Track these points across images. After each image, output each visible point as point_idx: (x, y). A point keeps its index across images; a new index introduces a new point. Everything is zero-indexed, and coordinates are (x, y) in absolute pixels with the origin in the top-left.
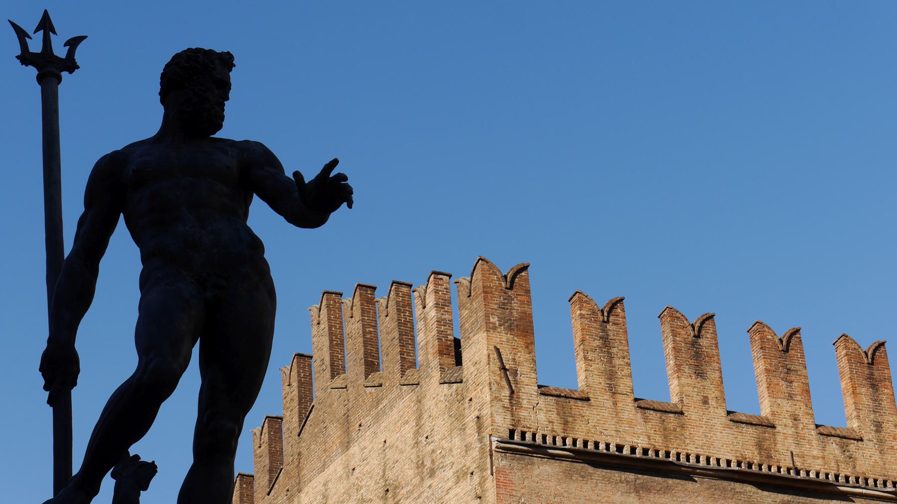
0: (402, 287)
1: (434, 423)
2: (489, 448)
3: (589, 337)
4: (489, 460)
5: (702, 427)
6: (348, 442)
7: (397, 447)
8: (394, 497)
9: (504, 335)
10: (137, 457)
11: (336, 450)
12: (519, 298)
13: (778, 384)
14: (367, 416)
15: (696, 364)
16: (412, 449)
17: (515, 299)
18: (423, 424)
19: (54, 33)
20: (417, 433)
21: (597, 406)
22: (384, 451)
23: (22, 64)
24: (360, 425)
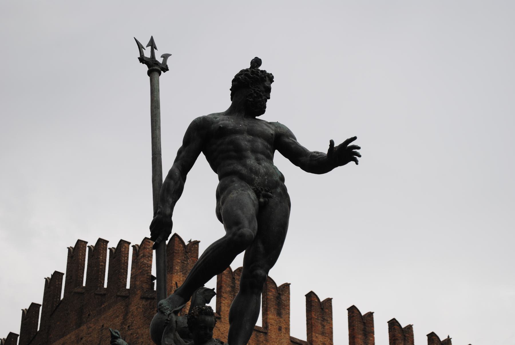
0: (126, 243)
1: (134, 319)
3: (225, 286)
5: (276, 343)
9: (182, 277)
12: (192, 259)
13: (317, 326)
15: (278, 309)
17: (190, 259)
19: (156, 49)
20: (123, 323)
21: (225, 323)
22: (102, 330)
23: (140, 63)
24: (89, 315)
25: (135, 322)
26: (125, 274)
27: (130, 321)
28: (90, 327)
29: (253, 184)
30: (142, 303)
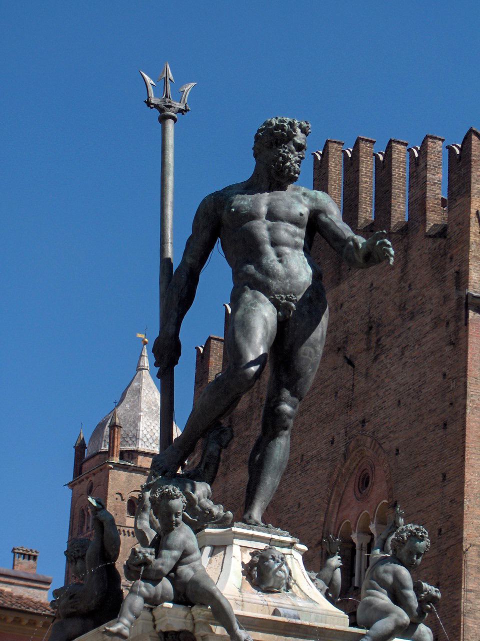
2: (464, 301)
4: (464, 312)
7: (383, 289)
8: (378, 333)
16: (396, 293)
20: (401, 279)
22: (371, 291)
28: (354, 286)
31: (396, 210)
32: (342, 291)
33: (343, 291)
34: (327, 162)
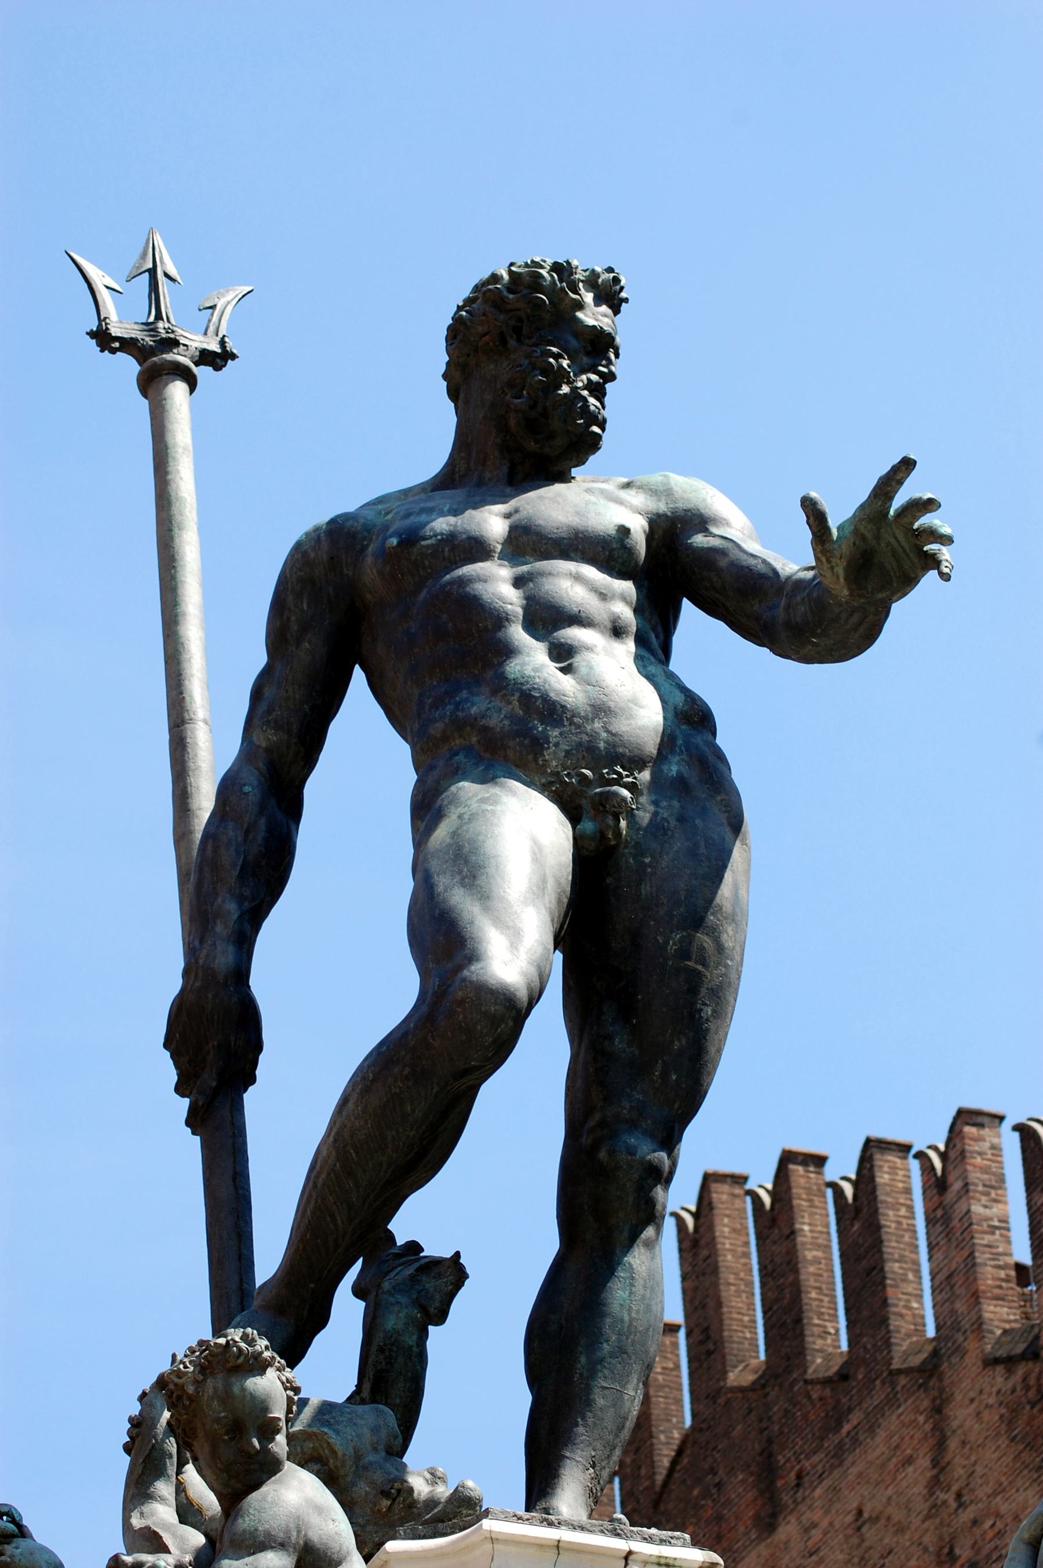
6: (774, 1515)
7: (889, 1518)
10: (414, 1247)
11: (746, 1534)
14: (815, 1453)
16: (923, 1522)
18: (948, 1463)
20: (935, 1484)
22: (859, 1529)
23: (102, 351)
24: (799, 1476)
25: (979, 1469)
26: (911, 1276)
27: (961, 1471)
28: (814, 1525)
29: (541, 763)
30: (992, 1386)
31: (901, 1315)
32: (785, 1543)
33: (787, 1543)
34: (711, 1228)
